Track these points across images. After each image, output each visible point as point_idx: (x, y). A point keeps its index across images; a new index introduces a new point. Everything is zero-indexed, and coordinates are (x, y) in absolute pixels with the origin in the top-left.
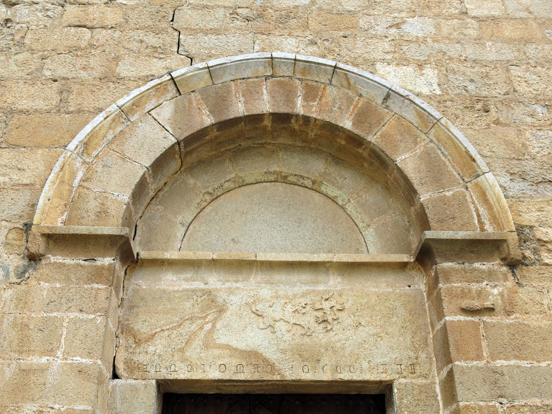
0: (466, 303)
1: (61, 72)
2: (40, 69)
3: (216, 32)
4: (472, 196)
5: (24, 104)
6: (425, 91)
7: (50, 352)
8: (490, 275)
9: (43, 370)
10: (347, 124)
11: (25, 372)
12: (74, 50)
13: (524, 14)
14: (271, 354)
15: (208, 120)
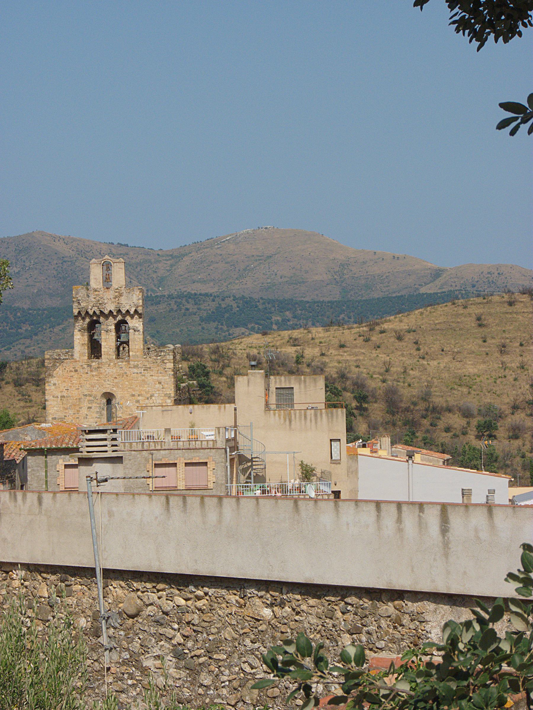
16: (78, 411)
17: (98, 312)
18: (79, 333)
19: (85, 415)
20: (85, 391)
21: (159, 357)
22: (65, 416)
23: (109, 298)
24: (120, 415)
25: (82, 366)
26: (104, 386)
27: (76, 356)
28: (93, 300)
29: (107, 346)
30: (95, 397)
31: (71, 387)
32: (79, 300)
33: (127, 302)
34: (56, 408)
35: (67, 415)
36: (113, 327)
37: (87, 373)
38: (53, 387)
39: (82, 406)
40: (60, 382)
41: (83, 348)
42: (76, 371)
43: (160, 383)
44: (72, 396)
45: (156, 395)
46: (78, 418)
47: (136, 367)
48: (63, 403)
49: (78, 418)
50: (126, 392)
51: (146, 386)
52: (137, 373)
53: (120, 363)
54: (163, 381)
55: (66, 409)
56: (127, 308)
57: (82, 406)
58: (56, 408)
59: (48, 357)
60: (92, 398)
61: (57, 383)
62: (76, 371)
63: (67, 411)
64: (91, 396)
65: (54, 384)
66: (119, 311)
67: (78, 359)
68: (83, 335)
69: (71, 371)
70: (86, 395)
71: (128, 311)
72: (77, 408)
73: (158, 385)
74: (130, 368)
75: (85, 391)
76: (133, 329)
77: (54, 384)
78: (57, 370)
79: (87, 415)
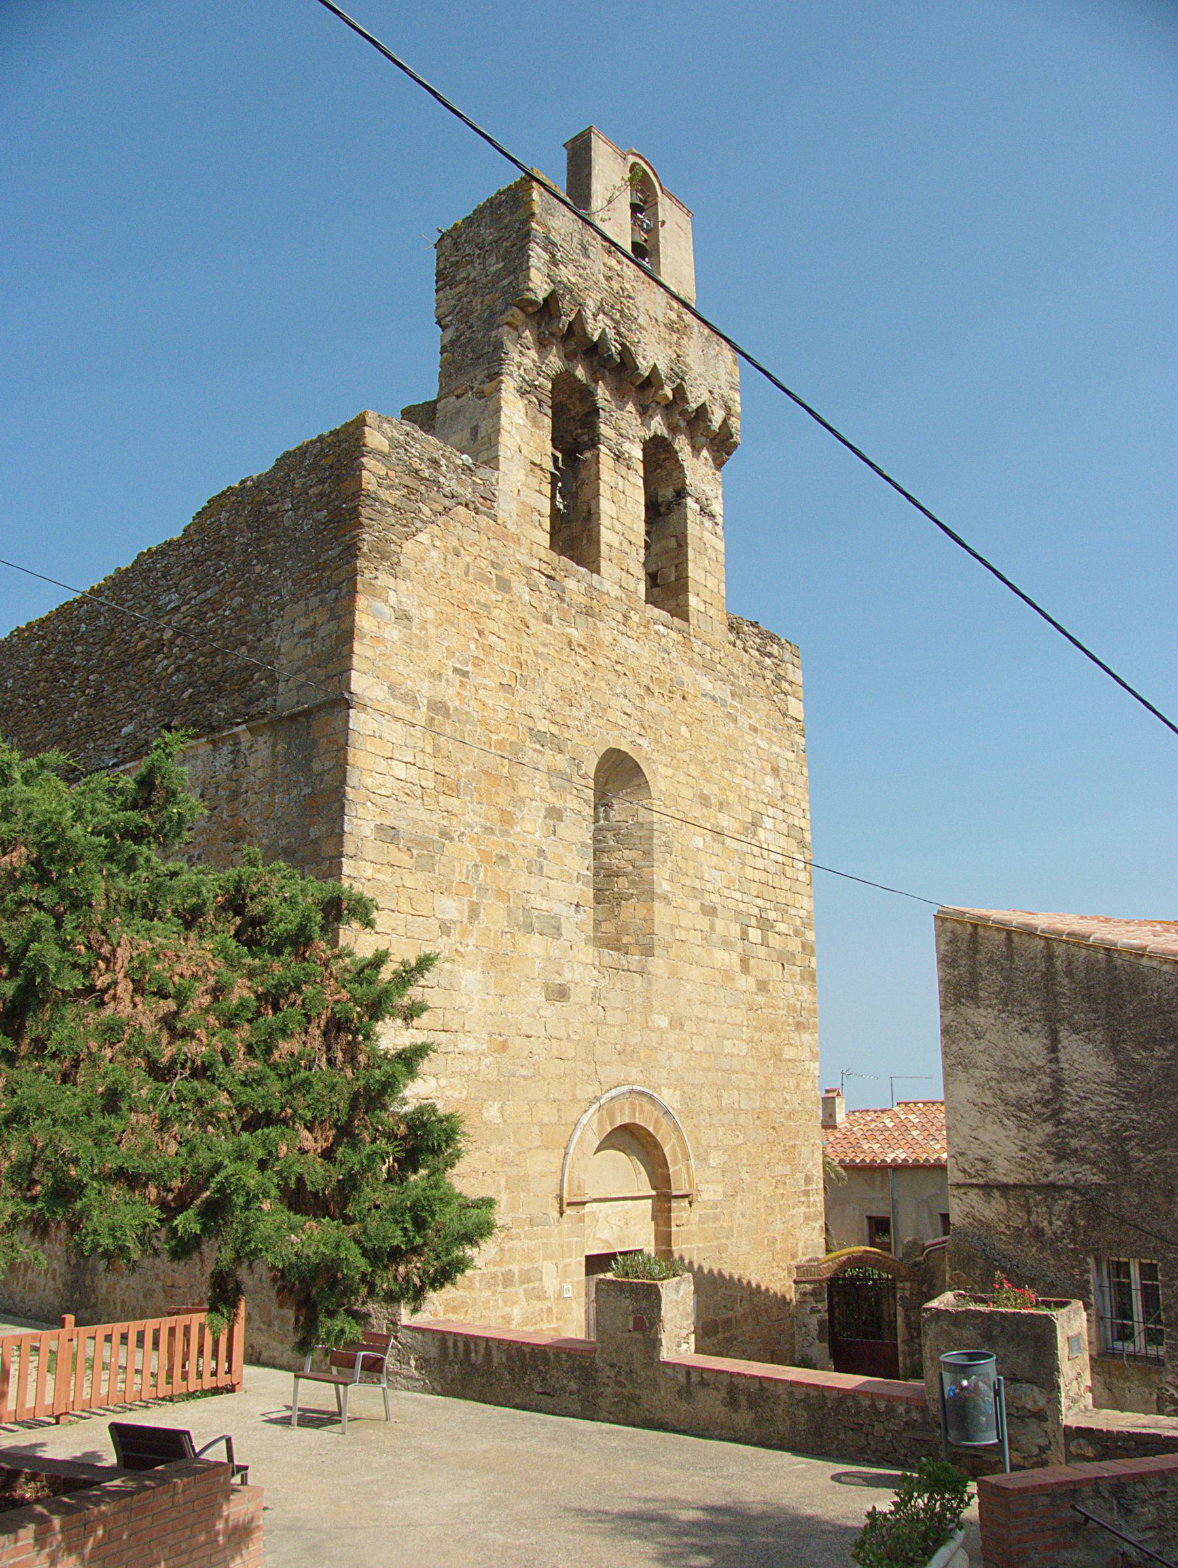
0: (679, 1223)
1: (557, 1096)
2: (548, 1094)
3: (608, 1063)
4: (684, 1170)
5: (545, 1121)
6: (675, 1106)
7: (570, 1256)
8: (684, 1209)
9: (570, 1264)
10: (651, 1130)
11: (565, 1266)
12: (559, 1077)
13: (710, 1050)
14: (611, 1241)
15: (610, 1129)
16: (507, 819)
17: (615, 347)
18: (521, 403)
19: (532, 853)
20: (538, 712)
21: (768, 661)
22: (444, 834)
23: (652, 313)
24: (666, 886)
25: (529, 570)
26: (610, 715)
27: (506, 507)
28: (603, 280)
29: (618, 526)
30: (576, 762)
31: (478, 662)
32: (555, 245)
33: (702, 369)
34: (400, 770)
35: (456, 827)
36: (637, 452)
37: (549, 621)
38: (394, 633)
39: (523, 791)
40: (430, 614)
41: (534, 483)
42: (504, 585)
43: (776, 771)
44: (483, 722)
45: (768, 822)
46: (503, 859)
47: (708, 668)
48: (437, 749)
49: (503, 859)
50: (681, 777)
51: (740, 770)
52: (713, 698)
53: (662, 629)
54: (782, 764)
55: (453, 791)
56: (705, 397)
57: (523, 791)
58: (400, 770)
59: (385, 446)
60: (562, 762)
61: (414, 611)
62: (504, 585)
63: (454, 804)
64: (561, 751)
65: (403, 617)
66: (679, 392)
67: (512, 528)
68: (534, 421)
69: (482, 578)
70: (540, 737)
71: (702, 411)
72: (503, 800)
73: (770, 781)
74: (691, 663)
75: (538, 712)
76: (697, 501)
77: (403, 617)
78: (423, 537)
79: (541, 852)
